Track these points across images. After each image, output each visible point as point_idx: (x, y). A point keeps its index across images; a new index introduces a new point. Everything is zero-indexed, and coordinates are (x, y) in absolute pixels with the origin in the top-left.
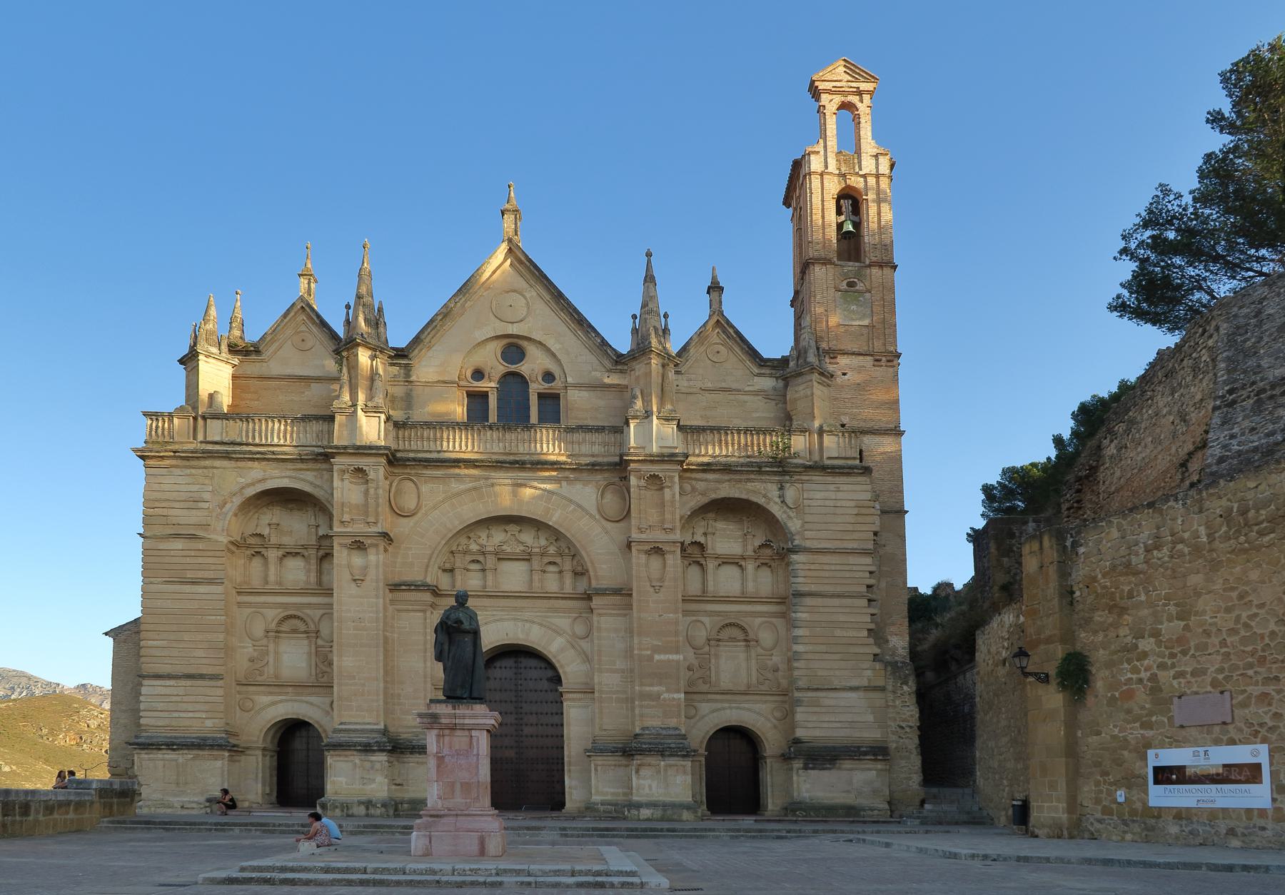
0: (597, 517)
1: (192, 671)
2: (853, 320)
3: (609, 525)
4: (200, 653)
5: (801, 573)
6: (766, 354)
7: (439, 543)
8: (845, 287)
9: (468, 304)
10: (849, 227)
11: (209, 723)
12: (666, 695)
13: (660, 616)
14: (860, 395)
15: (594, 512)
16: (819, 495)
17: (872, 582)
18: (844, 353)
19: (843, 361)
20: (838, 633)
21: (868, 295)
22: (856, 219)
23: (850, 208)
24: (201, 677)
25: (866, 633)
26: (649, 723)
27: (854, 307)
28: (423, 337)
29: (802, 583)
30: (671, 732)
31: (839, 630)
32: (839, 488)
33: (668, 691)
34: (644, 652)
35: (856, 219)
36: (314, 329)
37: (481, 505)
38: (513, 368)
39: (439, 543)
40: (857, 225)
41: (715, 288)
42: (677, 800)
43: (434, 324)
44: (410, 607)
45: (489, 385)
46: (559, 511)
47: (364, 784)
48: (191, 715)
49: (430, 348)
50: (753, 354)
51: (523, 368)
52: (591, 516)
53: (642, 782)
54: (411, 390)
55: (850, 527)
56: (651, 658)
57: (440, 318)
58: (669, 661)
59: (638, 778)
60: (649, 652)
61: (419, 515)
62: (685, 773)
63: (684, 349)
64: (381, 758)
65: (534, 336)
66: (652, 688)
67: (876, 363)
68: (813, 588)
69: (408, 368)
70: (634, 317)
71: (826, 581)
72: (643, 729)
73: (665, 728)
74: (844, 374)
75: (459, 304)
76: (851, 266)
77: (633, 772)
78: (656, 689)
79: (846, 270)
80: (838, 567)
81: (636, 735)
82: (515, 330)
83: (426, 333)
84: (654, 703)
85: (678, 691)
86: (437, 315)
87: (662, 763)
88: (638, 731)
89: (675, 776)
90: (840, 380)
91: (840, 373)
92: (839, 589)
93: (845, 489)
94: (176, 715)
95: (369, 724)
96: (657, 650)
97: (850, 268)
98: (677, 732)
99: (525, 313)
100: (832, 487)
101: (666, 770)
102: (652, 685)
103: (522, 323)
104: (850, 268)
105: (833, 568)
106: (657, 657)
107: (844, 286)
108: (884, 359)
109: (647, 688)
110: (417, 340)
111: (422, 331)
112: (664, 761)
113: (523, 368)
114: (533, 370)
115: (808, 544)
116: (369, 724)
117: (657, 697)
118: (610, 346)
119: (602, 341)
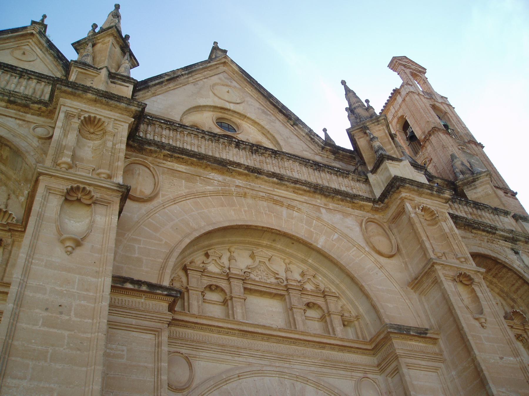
0: (367, 249)
3: (382, 260)
7: (181, 241)
28: (151, 84)
36: (38, 51)
37: (233, 213)
39: (181, 241)
43: (162, 80)
44: (134, 321)
51: (238, 136)
52: (359, 248)
57: (167, 78)
61: (155, 203)
65: (248, 115)
67: (505, 194)
83: (154, 83)
86: (166, 74)
103: (238, 106)
118: (317, 136)
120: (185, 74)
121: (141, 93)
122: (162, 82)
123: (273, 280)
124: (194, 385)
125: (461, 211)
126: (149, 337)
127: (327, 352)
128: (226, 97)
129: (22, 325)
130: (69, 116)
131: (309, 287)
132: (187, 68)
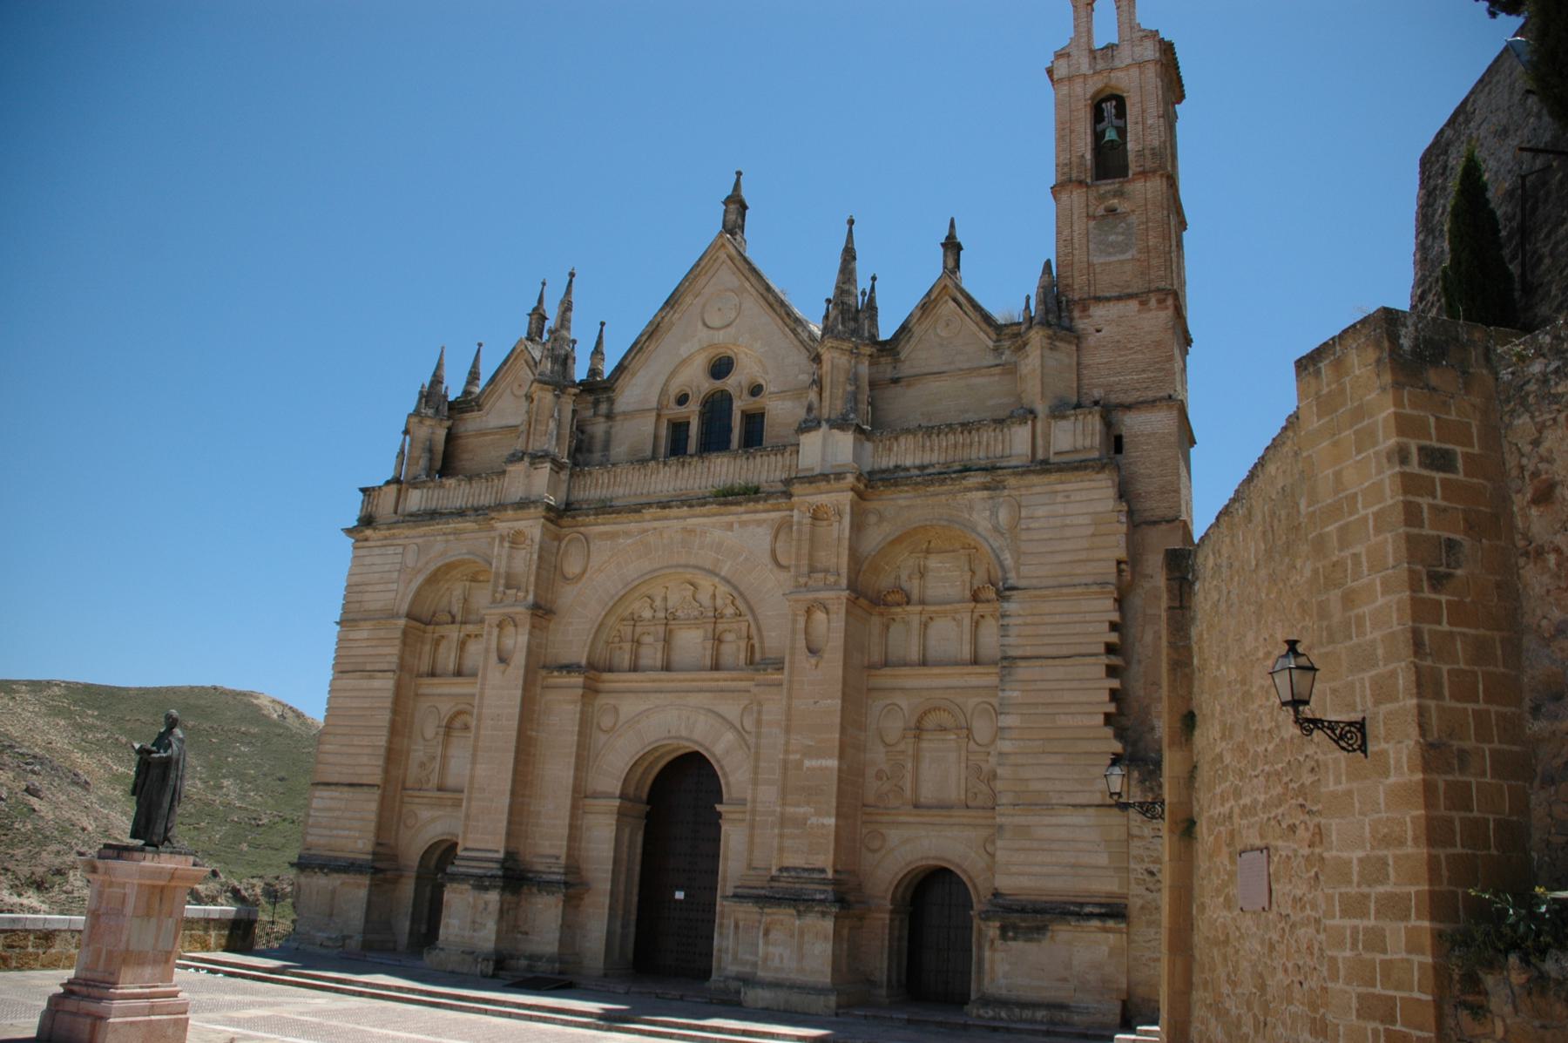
0: (770, 566)
1: (355, 780)
2: (1110, 254)
4: (365, 760)
5: (1013, 631)
6: (1000, 316)
8: (1103, 212)
9: (676, 316)
10: (1111, 135)
11: (360, 844)
12: (813, 820)
13: (815, 703)
14: (1120, 356)
15: (767, 559)
16: (1041, 512)
17: (1113, 638)
18: (1098, 299)
19: (1099, 312)
20: (1063, 720)
21: (1133, 219)
22: (1120, 123)
23: (1113, 111)
24: (361, 785)
25: (1100, 719)
26: (790, 861)
27: (1112, 238)
28: (626, 363)
29: (1018, 644)
30: (816, 875)
31: (1063, 717)
32: (1068, 497)
33: (818, 813)
34: (792, 757)
35: (1120, 123)
38: (718, 384)
40: (1122, 132)
41: (952, 246)
42: (811, 979)
43: (639, 346)
45: (692, 412)
46: (729, 563)
47: (474, 931)
48: (346, 833)
49: (633, 375)
50: (987, 318)
53: (771, 949)
54: (611, 427)
55: (1083, 555)
56: (799, 764)
57: (644, 338)
58: (822, 769)
59: (766, 943)
60: (798, 756)
61: (584, 580)
62: (826, 938)
63: (904, 329)
64: (493, 897)
66: (797, 810)
68: (1029, 652)
69: (611, 401)
70: (828, 301)
71: (1046, 640)
72: (781, 869)
73: (805, 870)
74: (1098, 331)
75: (666, 319)
76: (1107, 186)
77: (761, 934)
78: (802, 810)
79: (1102, 190)
80: (1065, 618)
81: (773, 879)
82: (721, 338)
83: (630, 358)
84: (796, 831)
85: (829, 815)
86: (641, 335)
87: (797, 922)
88: (774, 872)
89: (813, 944)
90: (1092, 340)
91: (1092, 330)
92: (1064, 651)
93: (1078, 498)
94: (335, 832)
95: (490, 851)
96: (808, 752)
97: (1109, 188)
98: (823, 876)
99: (733, 316)
100: (1060, 498)
101: (802, 934)
102: (798, 805)
103: (729, 329)
104: (1109, 188)
105: (1057, 618)
106: (807, 763)
107: (1100, 211)
108: (1153, 302)
109: (790, 810)
110: (621, 368)
111: (625, 357)
112: (799, 919)
113: (729, 382)
114: (740, 383)
115: (1023, 583)
116: (490, 851)
117: (801, 822)
119: (809, 337)
120: (668, 312)
121: (620, 381)
122: (641, 348)
123: (696, 613)
124: (617, 727)
125: (932, 450)
126: (572, 707)
127: (721, 684)
128: (716, 322)
129: (482, 732)
130: (502, 538)
131: (729, 611)
132: (667, 303)
